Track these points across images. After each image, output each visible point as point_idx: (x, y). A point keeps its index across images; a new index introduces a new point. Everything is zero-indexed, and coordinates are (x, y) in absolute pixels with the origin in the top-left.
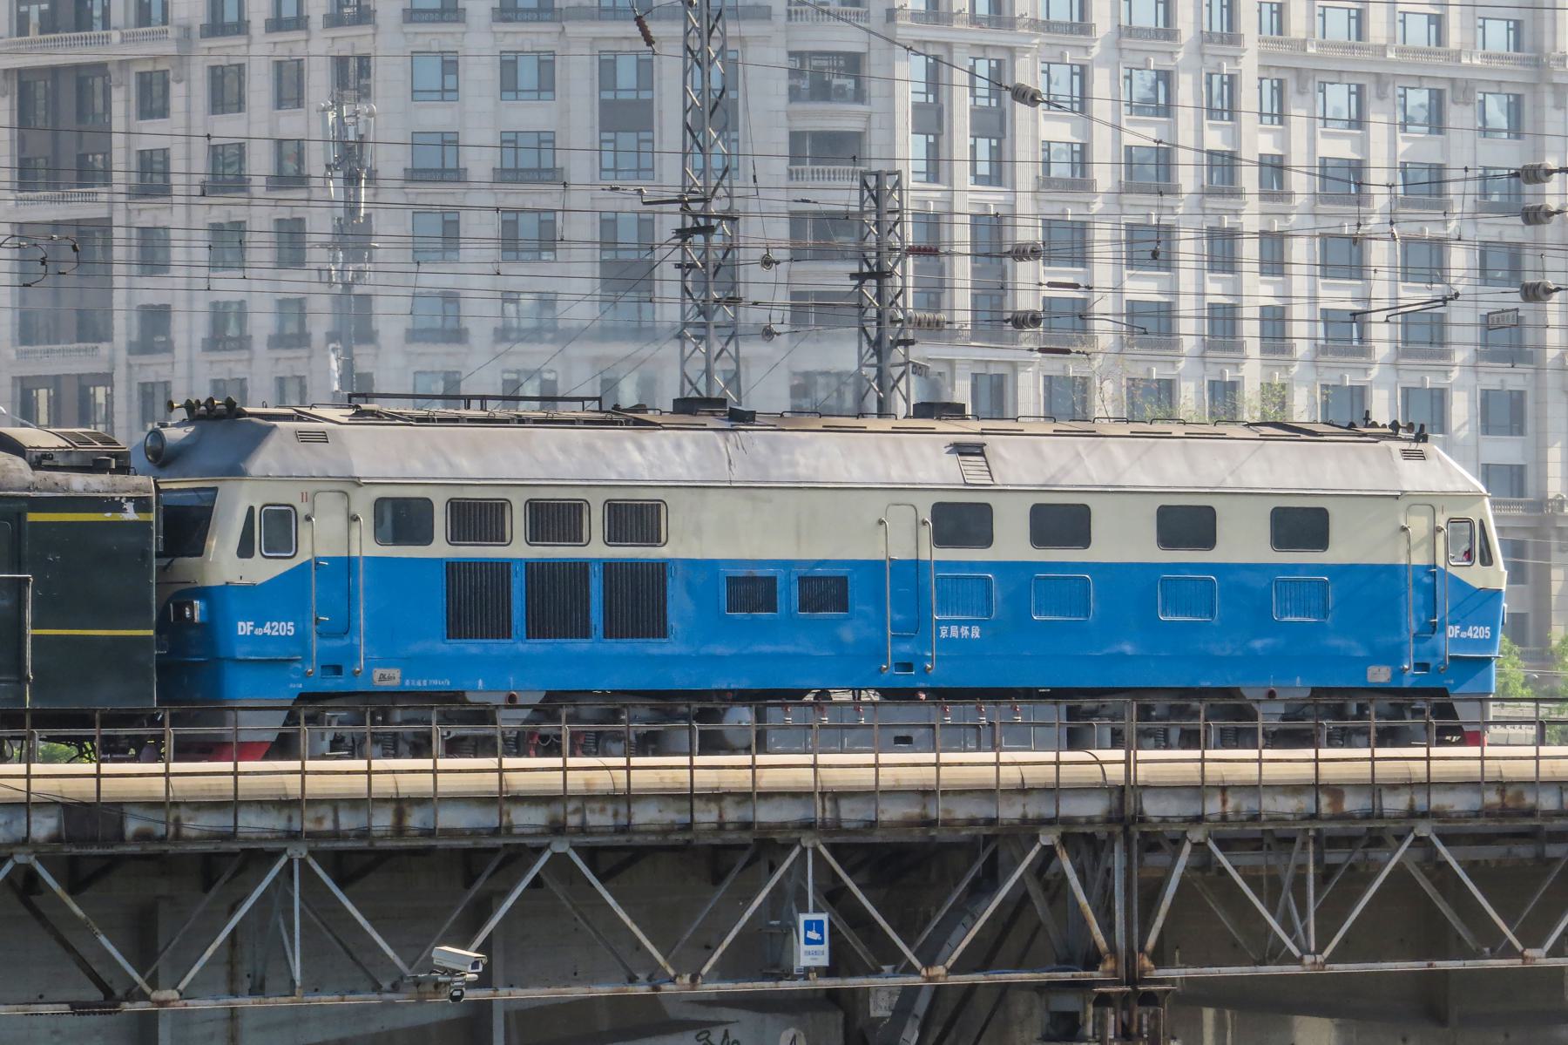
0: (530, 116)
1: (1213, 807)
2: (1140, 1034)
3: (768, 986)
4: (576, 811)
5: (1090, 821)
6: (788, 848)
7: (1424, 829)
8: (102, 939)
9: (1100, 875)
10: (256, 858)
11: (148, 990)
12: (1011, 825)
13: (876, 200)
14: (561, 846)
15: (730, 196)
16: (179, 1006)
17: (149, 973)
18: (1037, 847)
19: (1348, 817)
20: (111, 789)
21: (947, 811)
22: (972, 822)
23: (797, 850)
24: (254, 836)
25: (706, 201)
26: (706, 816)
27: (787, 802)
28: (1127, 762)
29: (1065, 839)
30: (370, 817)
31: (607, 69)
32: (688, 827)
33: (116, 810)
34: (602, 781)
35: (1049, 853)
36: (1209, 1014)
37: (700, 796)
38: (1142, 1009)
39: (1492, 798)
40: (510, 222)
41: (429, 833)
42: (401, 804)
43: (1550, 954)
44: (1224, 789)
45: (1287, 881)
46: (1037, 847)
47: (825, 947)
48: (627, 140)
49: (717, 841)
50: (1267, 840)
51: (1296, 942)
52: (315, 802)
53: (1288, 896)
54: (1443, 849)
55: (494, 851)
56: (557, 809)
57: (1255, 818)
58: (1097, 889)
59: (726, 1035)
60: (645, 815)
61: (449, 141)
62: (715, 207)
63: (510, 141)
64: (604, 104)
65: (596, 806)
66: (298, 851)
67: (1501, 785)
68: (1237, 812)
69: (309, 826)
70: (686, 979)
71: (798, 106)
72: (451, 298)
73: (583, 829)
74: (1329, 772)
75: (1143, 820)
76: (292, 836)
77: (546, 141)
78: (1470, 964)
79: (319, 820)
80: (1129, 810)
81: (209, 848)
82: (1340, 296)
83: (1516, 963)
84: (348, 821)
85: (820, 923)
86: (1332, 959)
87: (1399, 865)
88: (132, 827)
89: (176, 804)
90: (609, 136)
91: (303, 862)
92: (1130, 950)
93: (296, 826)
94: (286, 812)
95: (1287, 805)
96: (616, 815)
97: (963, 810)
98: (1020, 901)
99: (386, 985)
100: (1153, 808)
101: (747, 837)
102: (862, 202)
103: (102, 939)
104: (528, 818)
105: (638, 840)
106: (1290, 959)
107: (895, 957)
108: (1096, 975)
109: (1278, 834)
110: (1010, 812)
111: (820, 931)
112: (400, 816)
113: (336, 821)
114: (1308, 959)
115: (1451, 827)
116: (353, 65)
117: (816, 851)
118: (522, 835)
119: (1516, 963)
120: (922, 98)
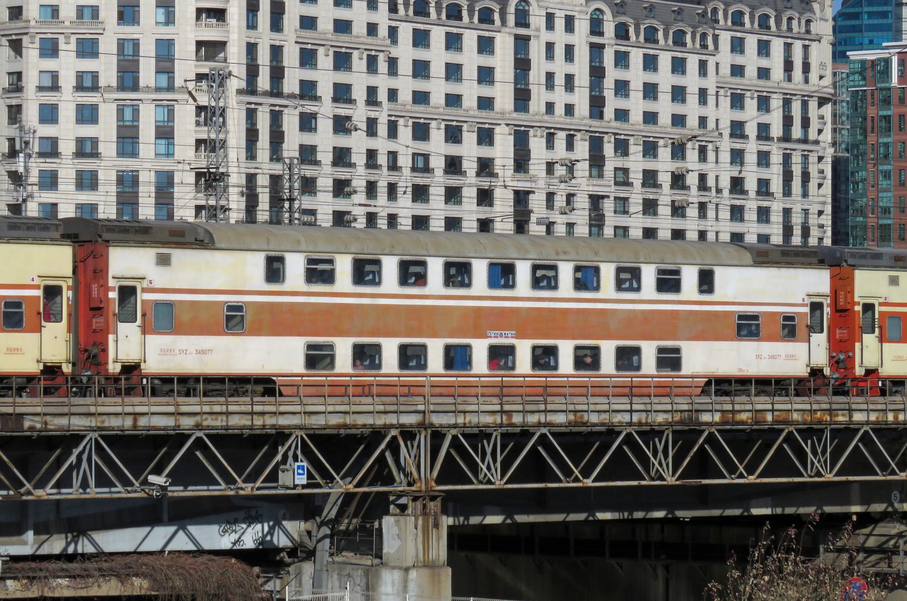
0: (87, 131)
1: (460, 420)
3: (282, 492)
4: (206, 419)
5: (411, 426)
6: (290, 435)
7: (544, 430)
8: (15, 470)
10: (75, 438)
13: (290, 169)
14: (200, 434)
15: (228, 167)
16: (46, 497)
17: (33, 483)
20: (19, 410)
21: (354, 421)
22: (364, 426)
24: (76, 428)
25: (217, 168)
26: (258, 421)
27: (290, 416)
29: (403, 433)
30: (123, 421)
31: (120, 111)
32: (251, 428)
33: (21, 415)
34: (217, 409)
35: (394, 438)
36: (451, 506)
37: (255, 413)
38: (432, 503)
39: (571, 417)
40: (80, 174)
42: (135, 414)
43: (594, 481)
44: (465, 412)
45: (489, 450)
47: (305, 476)
48: (130, 140)
49: (258, 432)
51: (492, 475)
52: (100, 414)
53: (489, 458)
55: (171, 436)
56: (198, 418)
59: (257, 512)
60: (235, 421)
61: (54, 141)
62: (221, 170)
63: (80, 141)
64: (118, 126)
65: (214, 417)
66: (96, 435)
67: (575, 412)
68: (470, 422)
69: (99, 425)
71: (198, 129)
72: (55, 205)
74: (507, 408)
75: (432, 425)
77: (95, 141)
78: (561, 485)
79: (103, 422)
80: (427, 422)
82: (484, 213)
84: (115, 422)
85: (303, 466)
86: (506, 483)
88: (27, 424)
89: (45, 414)
90: (121, 140)
91: (96, 440)
93: (93, 424)
94: (89, 419)
95: (488, 419)
96: (222, 421)
97: (361, 420)
98: (382, 458)
101: (274, 431)
102: (284, 170)
103: (15, 470)
104: (187, 422)
106: (489, 482)
107: (332, 479)
108: (413, 488)
110: (380, 421)
111: (303, 470)
112: (135, 420)
114: (498, 483)
116: (14, 110)
117: (302, 437)
119: (580, 485)
120: (249, 126)
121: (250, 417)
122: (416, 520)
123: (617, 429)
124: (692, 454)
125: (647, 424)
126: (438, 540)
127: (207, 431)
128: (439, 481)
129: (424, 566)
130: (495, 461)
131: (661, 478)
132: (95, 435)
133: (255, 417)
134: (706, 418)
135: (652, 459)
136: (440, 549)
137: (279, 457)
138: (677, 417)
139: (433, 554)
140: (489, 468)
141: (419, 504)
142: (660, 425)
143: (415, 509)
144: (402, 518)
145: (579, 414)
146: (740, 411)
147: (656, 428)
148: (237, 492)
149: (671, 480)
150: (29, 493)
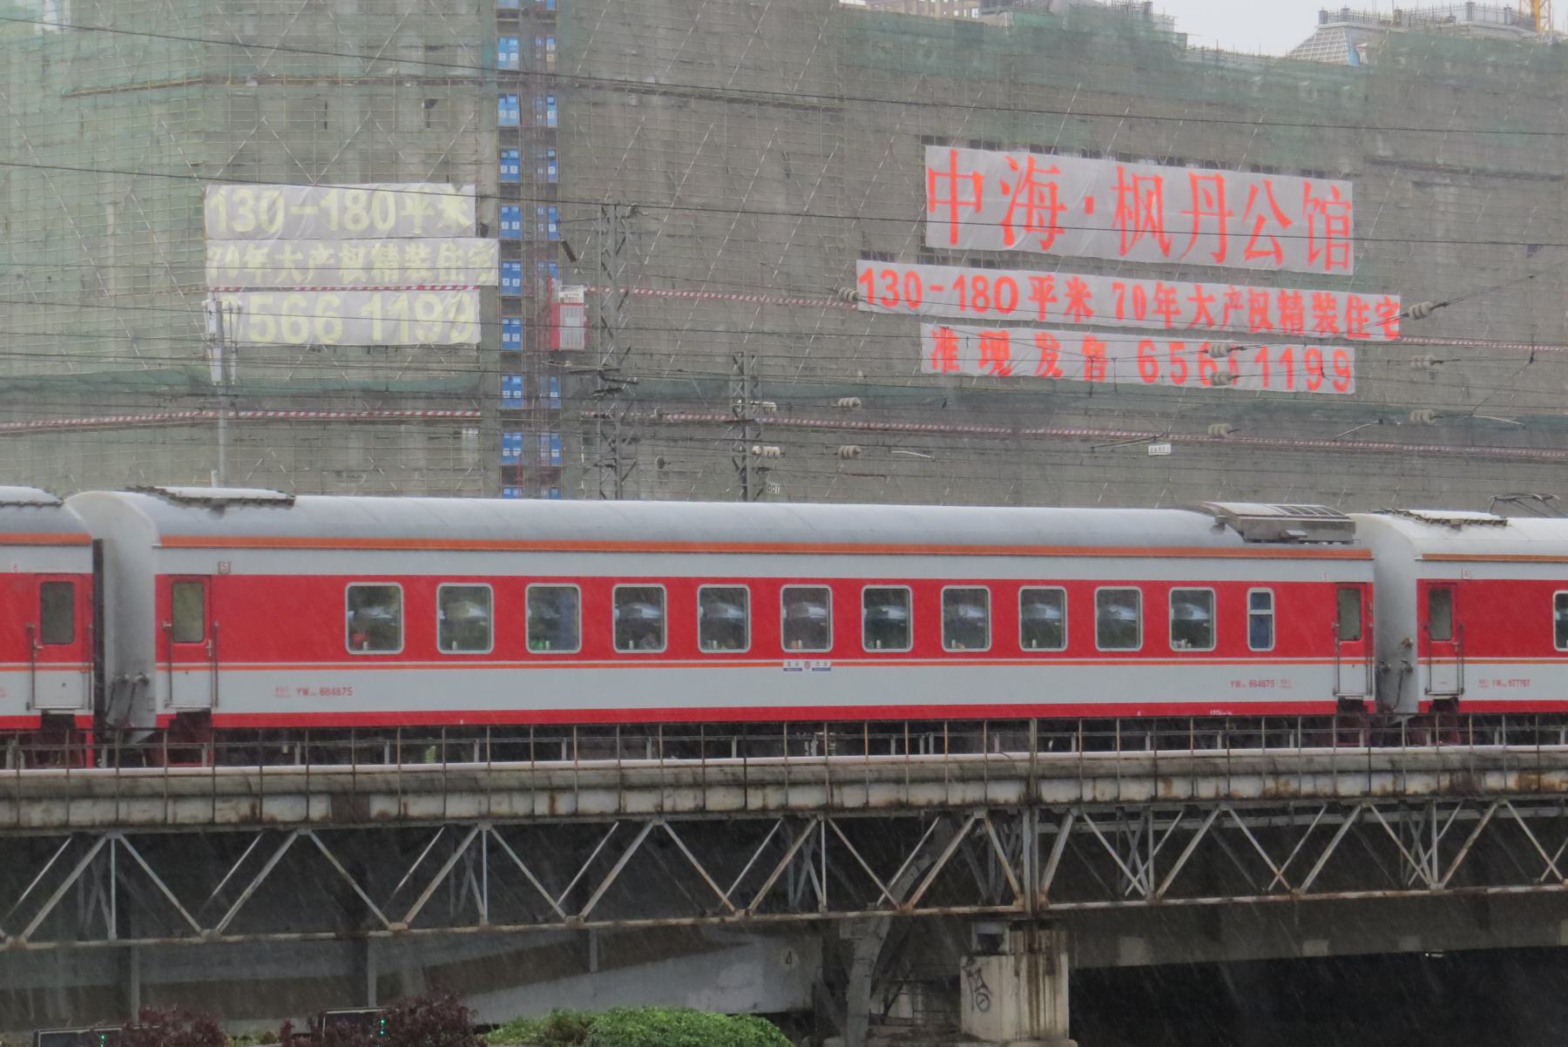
1: (1088, 795)
2: (1040, 949)
5: (1006, 803)
7: (1224, 807)
9: (1013, 838)
11: (385, 921)
12: (955, 806)
14: (661, 822)
18: (972, 820)
19: (1177, 800)
22: (929, 805)
23: (813, 823)
26: (755, 800)
28: (1031, 760)
32: (744, 809)
33: (367, 794)
35: (978, 823)
39: (1270, 784)
41: (575, 814)
42: (553, 790)
45: (1134, 843)
46: (972, 820)
50: (1119, 814)
51: (1140, 882)
54: (1237, 819)
57: (1117, 800)
58: (1009, 850)
65: (684, 792)
70: (742, 912)
73: (675, 812)
75: (1039, 801)
76: (483, 817)
79: (499, 804)
81: (427, 824)
83: (1286, 897)
84: (519, 806)
87: (1208, 831)
92: (1033, 893)
93: (484, 809)
99: (540, 918)
100: (1055, 793)
104: (639, 803)
105: (709, 817)
109: (1128, 809)
110: (958, 795)
112: (553, 800)
113: (511, 804)
115: (1239, 805)
118: (633, 814)
119: (1286, 897)
121: (740, 792)
122: (1018, 961)
123: (1344, 803)
124: (1470, 842)
125: (1395, 794)
126: (1055, 993)
127: (669, 818)
128: (1054, 895)
129: (1038, 1039)
130: (1144, 859)
131: (1420, 884)
132: (485, 827)
133: (750, 792)
134: (1493, 781)
135: (1404, 851)
136: (1057, 1011)
137: (789, 857)
138: (1445, 781)
139: (1045, 1018)
140: (1135, 871)
141: (1020, 933)
142: (1416, 795)
143: (1014, 940)
144: (994, 960)
145: (1282, 780)
146: (1550, 769)
147: (1410, 800)
148: (723, 921)
149: (1436, 885)
150: (382, 927)
